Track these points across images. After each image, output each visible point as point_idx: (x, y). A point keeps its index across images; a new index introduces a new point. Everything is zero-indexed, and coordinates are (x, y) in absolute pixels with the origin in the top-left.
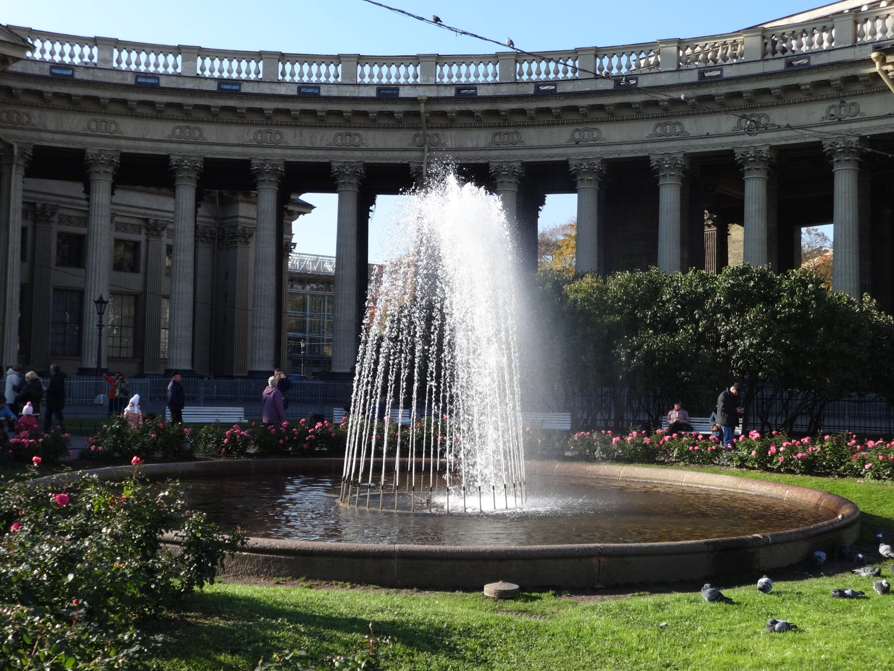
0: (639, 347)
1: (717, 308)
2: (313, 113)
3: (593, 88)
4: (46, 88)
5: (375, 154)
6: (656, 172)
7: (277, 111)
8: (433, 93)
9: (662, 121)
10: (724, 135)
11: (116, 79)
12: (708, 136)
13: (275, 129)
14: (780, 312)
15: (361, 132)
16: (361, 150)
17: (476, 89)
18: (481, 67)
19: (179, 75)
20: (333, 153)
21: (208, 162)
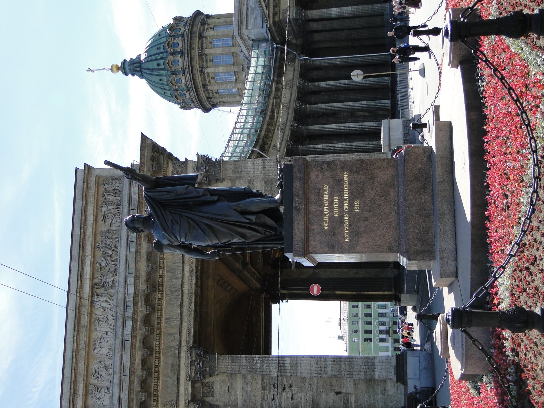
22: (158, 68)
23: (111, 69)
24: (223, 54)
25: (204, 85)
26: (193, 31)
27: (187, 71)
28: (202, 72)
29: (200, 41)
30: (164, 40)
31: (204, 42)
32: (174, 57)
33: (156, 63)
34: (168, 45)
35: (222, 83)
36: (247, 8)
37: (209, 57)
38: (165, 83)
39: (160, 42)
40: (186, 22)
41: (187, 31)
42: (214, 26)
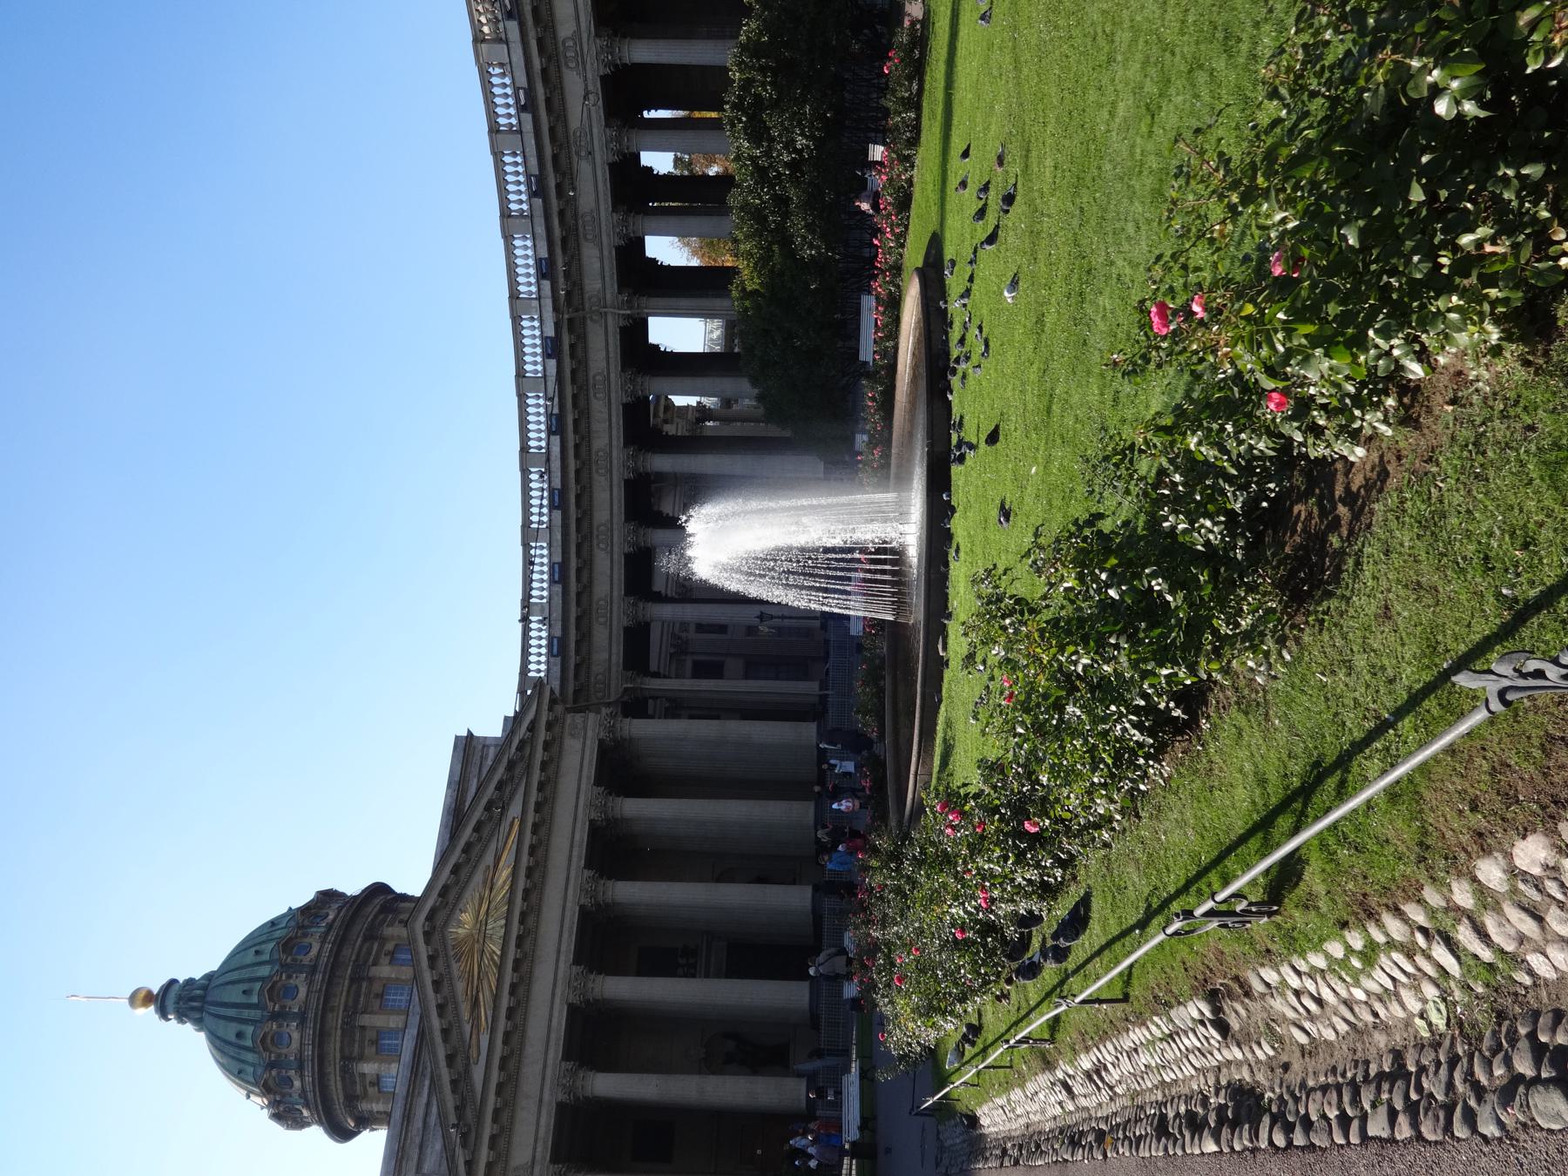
0: (804, 238)
1: (767, 154)
2: (576, 422)
3: (532, 135)
5: (612, 361)
6: (616, 66)
7: (577, 456)
8: (548, 303)
11: (558, 600)
14: (771, 94)
15: (591, 374)
16: (609, 373)
17: (541, 259)
18: (518, 252)
19: (550, 546)
20: (613, 401)
21: (628, 518)
23: (133, 1000)
28: (346, 1072)
29: (354, 987)
30: (265, 971)
31: (363, 989)
32: (280, 1026)
33: (233, 1028)
36: (428, 1104)
37: (371, 1035)
40: (330, 927)
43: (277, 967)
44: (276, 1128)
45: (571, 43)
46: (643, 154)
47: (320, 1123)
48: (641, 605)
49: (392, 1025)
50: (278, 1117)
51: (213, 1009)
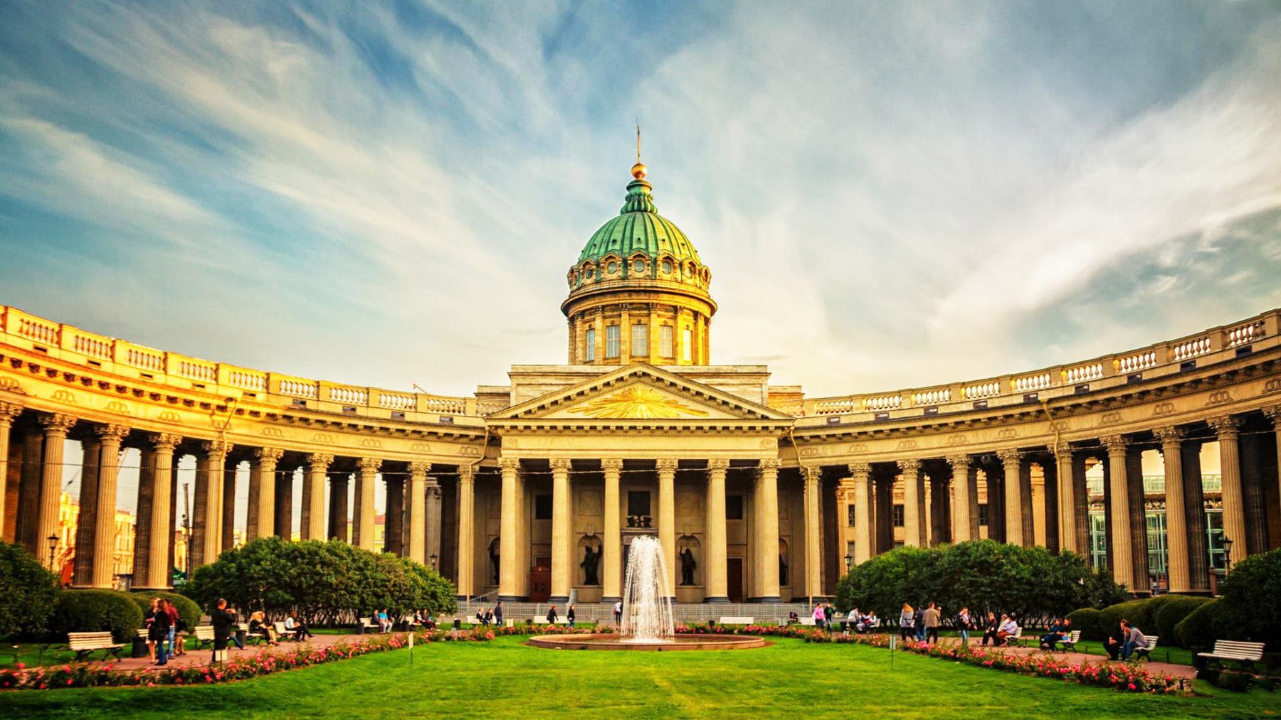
4: (822, 433)
7: (957, 423)
9: (1214, 392)
10: (1259, 398)
12: (1246, 400)
13: (960, 434)
15: (1016, 428)
20: (998, 444)
22: (612, 239)
24: (620, 341)
25: (583, 314)
26: (661, 295)
27: (597, 287)
28: (593, 311)
30: (652, 248)
32: (620, 266)
34: (639, 255)
35: (585, 342)
36: (551, 384)
37: (616, 320)
38: (591, 253)
39: (650, 242)
41: (660, 284)
42: (672, 327)
43: (653, 256)
44: (568, 270)
45: (1226, 397)
46: (1216, 445)
47: (570, 297)
48: (865, 474)
49: (622, 334)
50: (572, 271)
51: (631, 219)
